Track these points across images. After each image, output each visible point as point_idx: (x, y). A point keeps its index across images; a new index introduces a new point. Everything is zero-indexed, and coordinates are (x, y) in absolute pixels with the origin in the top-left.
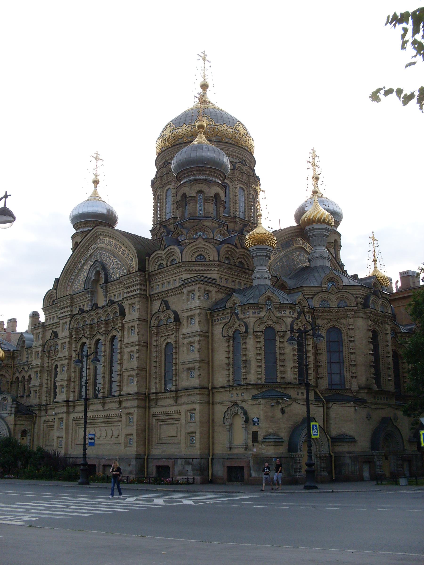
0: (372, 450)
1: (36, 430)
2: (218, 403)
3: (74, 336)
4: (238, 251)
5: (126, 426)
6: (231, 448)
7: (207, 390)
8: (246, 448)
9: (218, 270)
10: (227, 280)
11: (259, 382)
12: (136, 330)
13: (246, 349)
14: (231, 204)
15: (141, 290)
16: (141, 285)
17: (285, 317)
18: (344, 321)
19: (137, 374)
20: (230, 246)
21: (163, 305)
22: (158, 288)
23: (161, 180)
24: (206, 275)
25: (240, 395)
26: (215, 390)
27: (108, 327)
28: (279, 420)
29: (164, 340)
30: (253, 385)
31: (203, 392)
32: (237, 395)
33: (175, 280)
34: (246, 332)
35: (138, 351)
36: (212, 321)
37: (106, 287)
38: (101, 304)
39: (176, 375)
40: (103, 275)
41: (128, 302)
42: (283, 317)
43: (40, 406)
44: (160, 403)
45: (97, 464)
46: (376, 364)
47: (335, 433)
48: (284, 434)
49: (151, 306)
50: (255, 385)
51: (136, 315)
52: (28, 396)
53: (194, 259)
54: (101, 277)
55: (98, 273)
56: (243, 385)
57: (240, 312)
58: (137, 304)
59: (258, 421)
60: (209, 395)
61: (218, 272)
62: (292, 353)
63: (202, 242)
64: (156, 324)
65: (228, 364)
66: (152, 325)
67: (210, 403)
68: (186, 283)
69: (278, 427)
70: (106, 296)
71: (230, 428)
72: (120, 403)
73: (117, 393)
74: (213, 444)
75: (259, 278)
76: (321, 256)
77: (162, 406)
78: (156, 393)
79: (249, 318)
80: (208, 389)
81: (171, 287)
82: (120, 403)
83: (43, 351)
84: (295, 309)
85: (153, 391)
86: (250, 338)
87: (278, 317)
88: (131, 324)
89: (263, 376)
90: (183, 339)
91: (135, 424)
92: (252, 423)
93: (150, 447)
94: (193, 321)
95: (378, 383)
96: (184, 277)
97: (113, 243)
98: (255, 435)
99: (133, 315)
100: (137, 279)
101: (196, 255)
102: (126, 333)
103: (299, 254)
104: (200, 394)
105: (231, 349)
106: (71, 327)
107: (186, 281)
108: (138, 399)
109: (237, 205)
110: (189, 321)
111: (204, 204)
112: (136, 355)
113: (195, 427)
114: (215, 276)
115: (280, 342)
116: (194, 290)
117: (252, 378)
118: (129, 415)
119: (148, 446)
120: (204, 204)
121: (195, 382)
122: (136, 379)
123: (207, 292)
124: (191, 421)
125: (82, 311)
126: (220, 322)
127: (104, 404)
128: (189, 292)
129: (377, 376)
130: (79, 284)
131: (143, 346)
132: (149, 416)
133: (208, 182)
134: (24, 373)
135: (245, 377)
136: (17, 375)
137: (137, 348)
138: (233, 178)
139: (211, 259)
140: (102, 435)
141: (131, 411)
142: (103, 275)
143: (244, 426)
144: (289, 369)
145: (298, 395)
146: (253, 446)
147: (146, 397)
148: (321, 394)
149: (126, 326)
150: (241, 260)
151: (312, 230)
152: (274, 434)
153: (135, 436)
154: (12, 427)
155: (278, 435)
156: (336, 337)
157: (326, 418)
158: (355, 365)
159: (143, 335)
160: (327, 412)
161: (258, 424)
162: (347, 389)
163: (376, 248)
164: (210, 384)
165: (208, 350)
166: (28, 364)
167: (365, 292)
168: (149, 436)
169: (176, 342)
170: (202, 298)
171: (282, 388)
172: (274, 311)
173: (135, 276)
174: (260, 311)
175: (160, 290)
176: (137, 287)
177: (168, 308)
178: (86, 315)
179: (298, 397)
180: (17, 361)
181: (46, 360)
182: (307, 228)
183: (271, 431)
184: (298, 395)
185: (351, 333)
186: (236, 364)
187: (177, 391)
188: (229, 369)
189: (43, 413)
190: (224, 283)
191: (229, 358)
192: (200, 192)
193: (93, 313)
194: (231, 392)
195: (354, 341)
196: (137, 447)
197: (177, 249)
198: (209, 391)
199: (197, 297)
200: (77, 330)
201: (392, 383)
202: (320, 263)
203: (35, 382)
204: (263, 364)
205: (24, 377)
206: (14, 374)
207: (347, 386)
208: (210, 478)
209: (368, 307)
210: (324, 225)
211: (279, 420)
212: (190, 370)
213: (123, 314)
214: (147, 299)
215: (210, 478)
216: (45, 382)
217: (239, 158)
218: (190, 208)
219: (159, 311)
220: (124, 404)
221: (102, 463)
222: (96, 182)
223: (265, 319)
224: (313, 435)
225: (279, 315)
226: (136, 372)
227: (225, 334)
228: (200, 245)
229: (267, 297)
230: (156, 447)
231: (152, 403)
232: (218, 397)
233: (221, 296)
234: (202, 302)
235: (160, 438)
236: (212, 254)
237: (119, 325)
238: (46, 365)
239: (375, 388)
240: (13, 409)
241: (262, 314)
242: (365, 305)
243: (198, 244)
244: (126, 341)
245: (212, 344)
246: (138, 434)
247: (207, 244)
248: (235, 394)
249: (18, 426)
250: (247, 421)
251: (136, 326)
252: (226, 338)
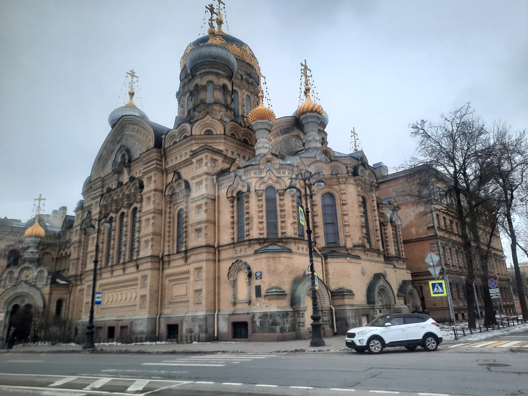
0: (368, 303)
1: (72, 298)
2: (224, 260)
3: (103, 212)
4: (242, 129)
5: (141, 288)
6: (234, 304)
7: (213, 248)
8: (250, 303)
9: (224, 143)
10: (233, 153)
11: (262, 237)
12: (152, 199)
13: (248, 208)
14: (240, 107)
15: (157, 164)
16: (157, 160)
17: (285, 177)
18: (336, 187)
19: (152, 239)
20: (235, 123)
21: (176, 176)
22: (173, 161)
24: (214, 147)
25: (243, 251)
26: (221, 248)
27: (130, 201)
28: (281, 273)
29: (177, 207)
30: (256, 239)
31: (210, 250)
32: (241, 251)
33: (186, 153)
34: (249, 191)
35: (153, 218)
36: (218, 186)
37: (129, 167)
38: (124, 183)
39: (186, 237)
40: (127, 157)
41: (146, 177)
42: (283, 177)
43: (75, 276)
44: (173, 264)
45: (116, 326)
46: (366, 225)
48: (287, 288)
49: (166, 178)
50: (258, 241)
51: (152, 186)
52: (68, 269)
53: (203, 133)
54: (128, 161)
55: (123, 156)
56: (247, 240)
57: (243, 175)
58: (153, 177)
59: (261, 275)
60: (215, 253)
62: (291, 210)
63: (210, 119)
64: (170, 193)
65: (233, 223)
66: (166, 194)
67: (216, 261)
68: (194, 154)
70: (129, 175)
71: (234, 284)
72: (137, 267)
73: (135, 258)
74: (219, 300)
75: (260, 148)
76: (314, 139)
77: (174, 267)
78: (169, 255)
79: (250, 178)
80: (214, 247)
81: (183, 159)
82: (137, 267)
83: (81, 229)
84: (293, 170)
85: (166, 253)
86: (252, 197)
87: (277, 177)
88: (148, 195)
89: (265, 231)
90: (192, 203)
91: (148, 285)
92: (255, 278)
93: (163, 307)
94: (201, 186)
95: (369, 242)
96: (194, 148)
98: (258, 289)
99: (149, 187)
100: (154, 155)
101: (205, 130)
102: (144, 203)
103: (295, 140)
104: (207, 252)
105: (235, 208)
106: (101, 204)
107: (195, 152)
108: (152, 262)
109: (245, 108)
110: (197, 187)
111: (213, 92)
112: (152, 222)
113: (202, 285)
114: (221, 147)
115: (280, 200)
116: (202, 159)
117: (255, 234)
118: (145, 277)
119: (161, 306)
120: (213, 92)
121: (202, 241)
122: (150, 244)
123: (214, 161)
124: (199, 279)
125: (109, 190)
126: (225, 185)
127: (124, 269)
128: (198, 161)
129: (368, 236)
130: (109, 169)
131: (158, 213)
132: (162, 278)
133: (217, 74)
134: (66, 250)
135: (247, 233)
136: (62, 252)
137: (152, 215)
139: (218, 133)
141: (146, 273)
142: (127, 157)
143: (247, 281)
144: (289, 225)
145: (299, 249)
146: (257, 300)
147: (160, 259)
148: (320, 251)
149: (144, 197)
150: (246, 138)
151: (306, 118)
152: (277, 288)
153: (148, 297)
154: (47, 297)
155: (280, 289)
156: (331, 200)
157: (326, 273)
158: (349, 225)
159: (158, 204)
160: (326, 267)
161: (261, 278)
162: (342, 247)
163: (357, 141)
164: (216, 242)
165: (215, 211)
166: (68, 242)
167: (355, 163)
168: (162, 296)
169: (187, 207)
170: (209, 165)
171: (283, 243)
172: (274, 172)
173: (152, 152)
174: (261, 173)
175: (174, 163)
176: (154, 162)
177: (180, 177)
178: (113, 193)
179: (298, 251)
180: (62, 240)
181: (83, 236)
182: (301, 117)
183: (274, 285)
184: (299, 249)
185: (344, 197)
186: (240, 221)
187: (186, 251)
188: (233, 228)
189: (79, 283)
190: (229, 155)
191: (233, 217)
192: (210, 82)
193: (119, 190)
194: (235, 249)
195: (346, 204)
196: (149, 308)
197: (188, 126)
198: (215, 249)
199: (204, 164)
200: (105, 206)
201: (380, 243)
202: (312, 145)
203: (74, 256)
204: (264, 220)
205: (66, 253)
206: (59, 251)
207: (342, 244)
208: (216, 335)
209: (358, 175)
210: (315, 114)
211: (281, 273)
212: (198, 230)
213: (142, 187)
214: (162, 172)
215: (216, 335)
216: (81, 255)
218: (202, 95)
219: (172, 181)
220: (141, 267)
221: (120, 325)
222: (132, 94)
223: (266, 179)
225: (279, 175)
226: (151, 237)
227: (229, 195)
228: (208, 122)
229: (268, 158)
230: (168, 306)
231: (166, 266)
232: (224, 254)
233: (226, 166)
235: (172, 297)
236: (219, 129)
237: (139, 197)
238: (83, 240)
239: (368, 246)
241: (263, 175)
242: (355, 174)
243: (206, 121)
244: (144, 210)
245: (218, 206)
246: (151, 295)
247: (214, 120)
248: (239, 250)
249: (54, 296)
250: (250, 275)
251: (152, 197)
252: (230, 199)
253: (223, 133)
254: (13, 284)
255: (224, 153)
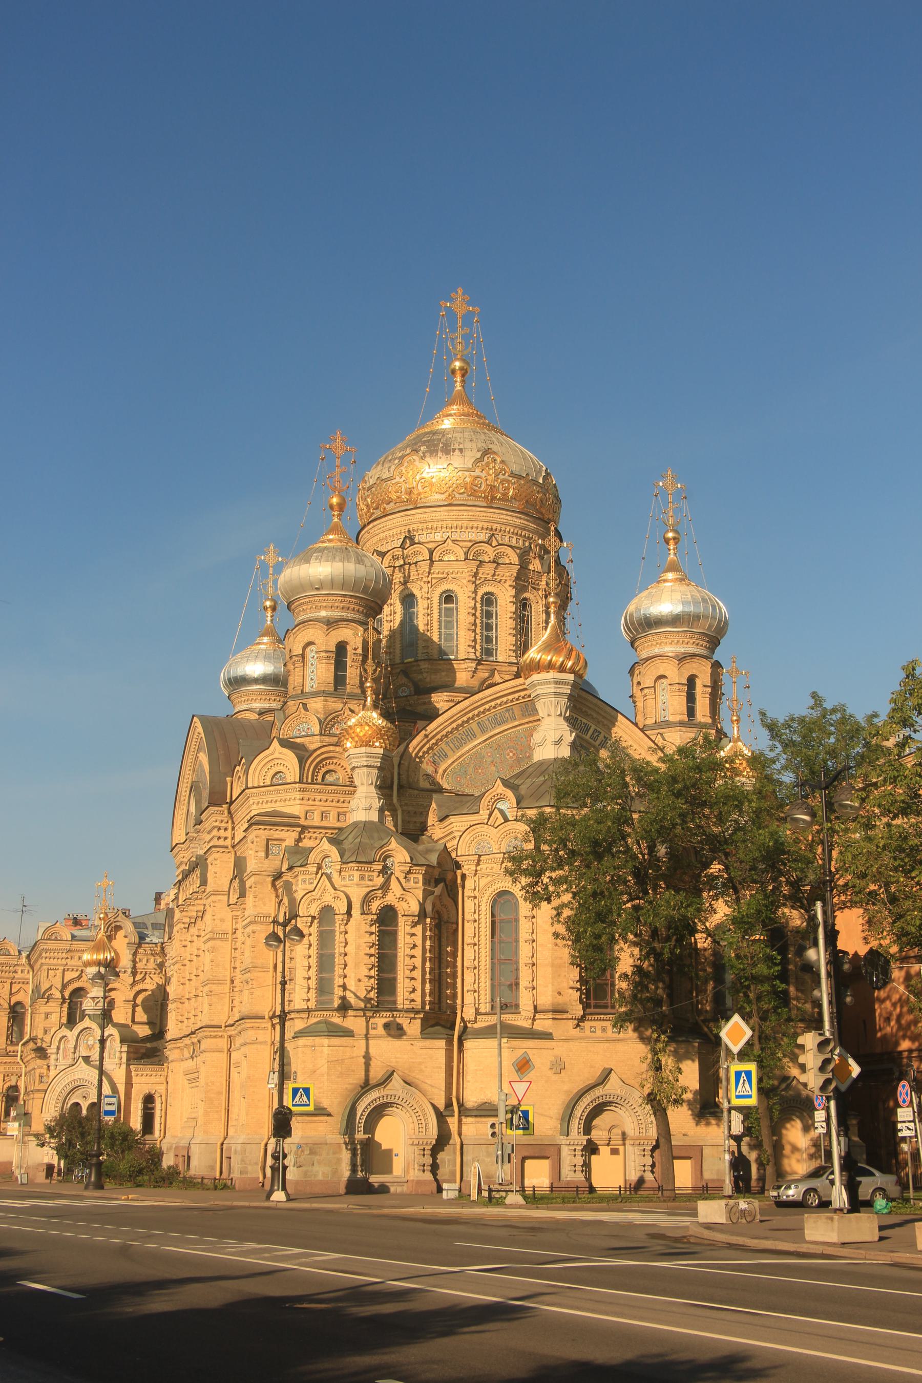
17: (351, 886)
28: (323, 1075)
47: (475, 1100)
61: (304, 802)
62: (362, 953)
69: (320, 1088)
101: (272, 772)
114: (295, 809)
138: (464, 578)
154: (121, 1088)
159: (222, 920)
217: (487, 529)
224: (737, 1097)
225: (343, 883)
228: (276, 755)
234: (261, 863)
240: (124, 1056)
254: (70, 1062)
255: (302, 822)
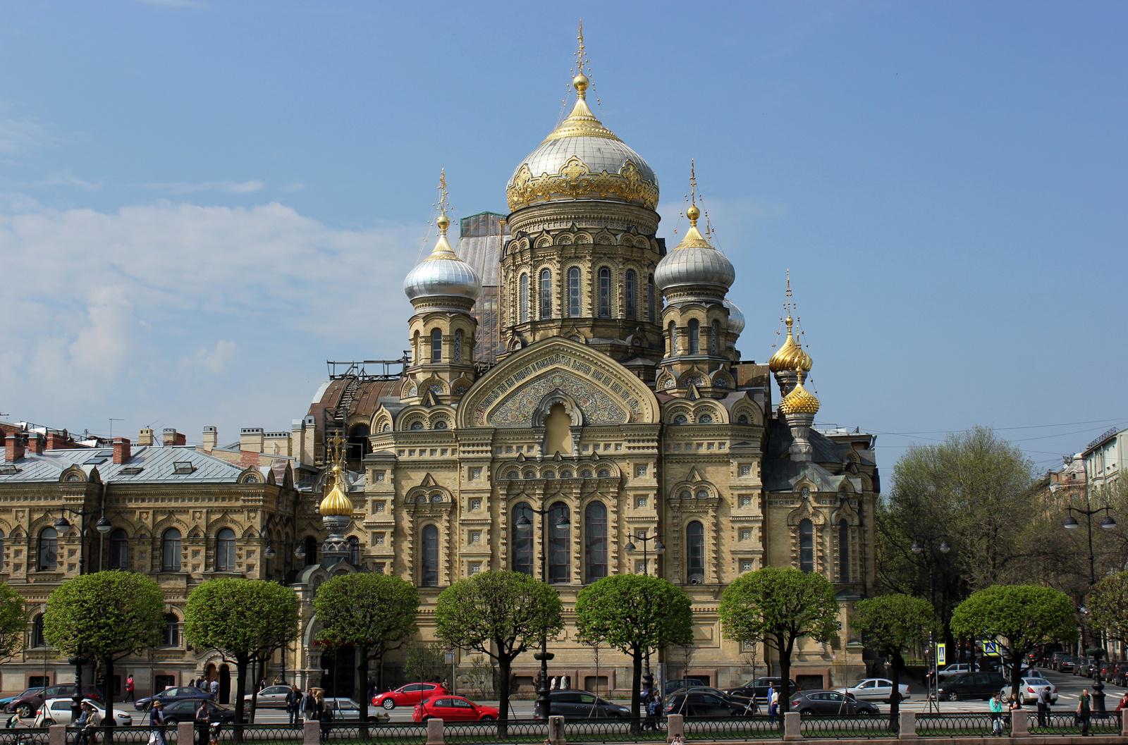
23: (563, 250)
29: (688, 517)
97: (589, 369)
101: (739, 415)
139: (756, 422)
140: (569, 636)
183: (853, 637)
230: (675, 652)
253: (762, 424)
